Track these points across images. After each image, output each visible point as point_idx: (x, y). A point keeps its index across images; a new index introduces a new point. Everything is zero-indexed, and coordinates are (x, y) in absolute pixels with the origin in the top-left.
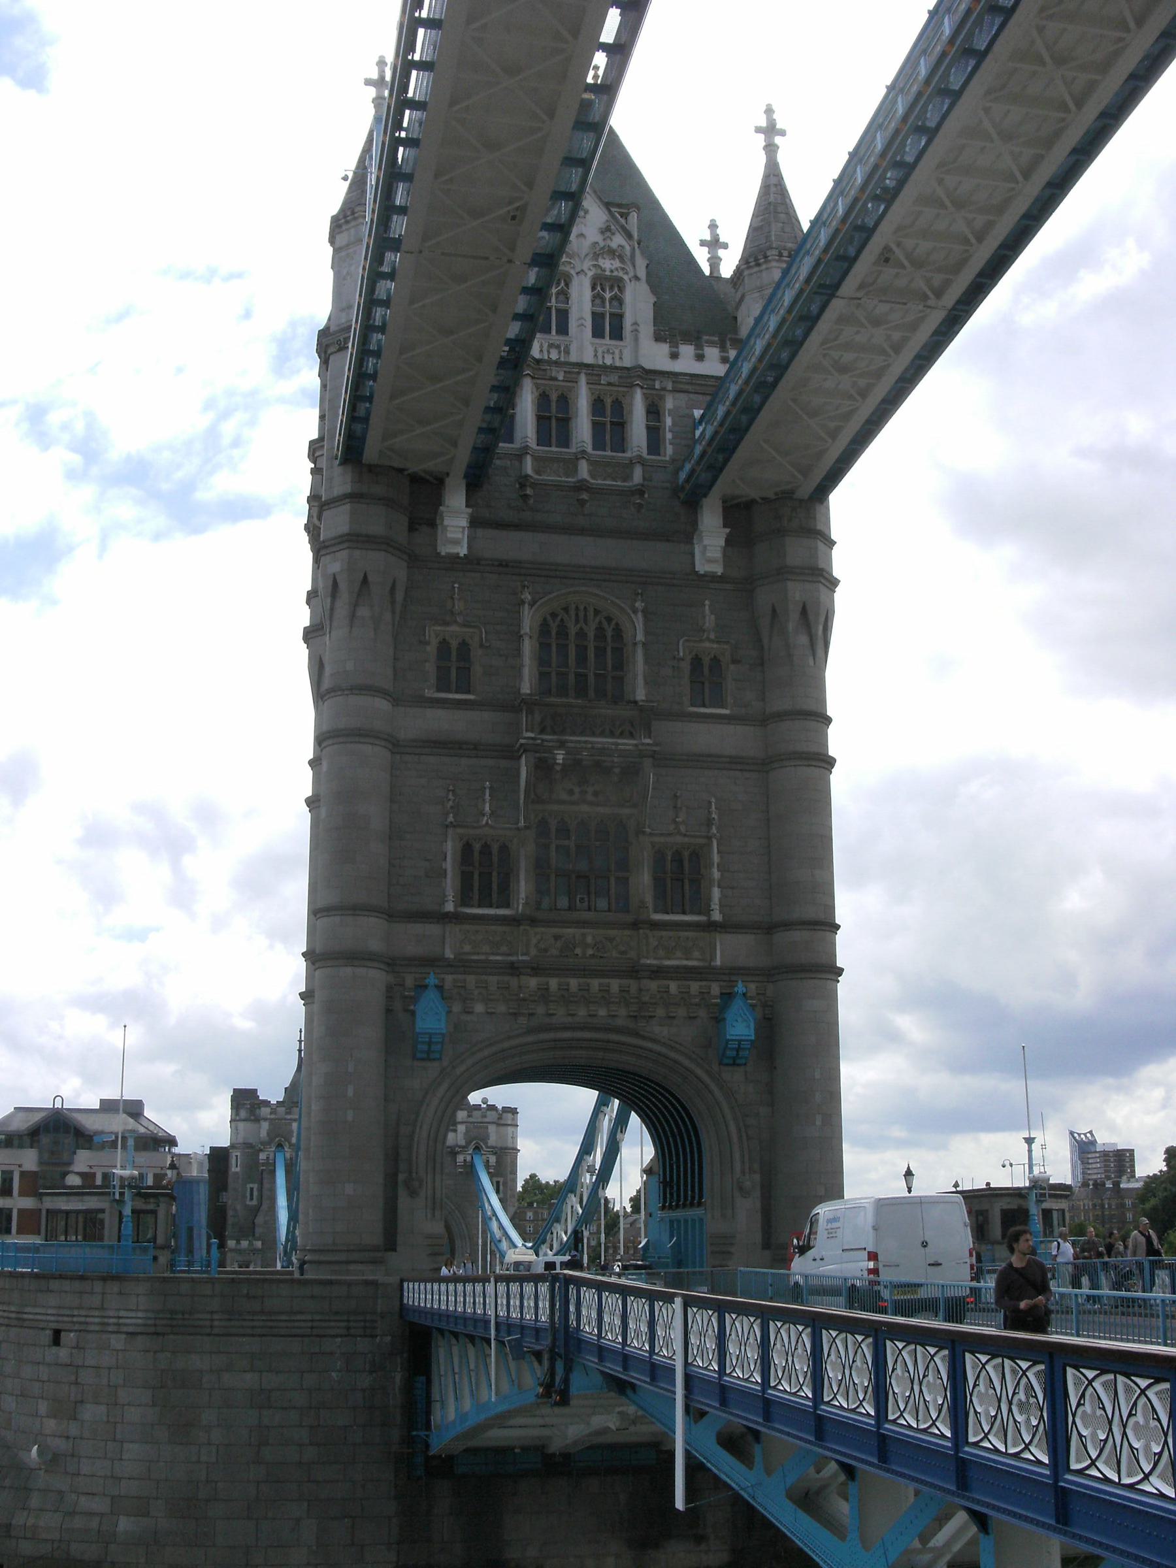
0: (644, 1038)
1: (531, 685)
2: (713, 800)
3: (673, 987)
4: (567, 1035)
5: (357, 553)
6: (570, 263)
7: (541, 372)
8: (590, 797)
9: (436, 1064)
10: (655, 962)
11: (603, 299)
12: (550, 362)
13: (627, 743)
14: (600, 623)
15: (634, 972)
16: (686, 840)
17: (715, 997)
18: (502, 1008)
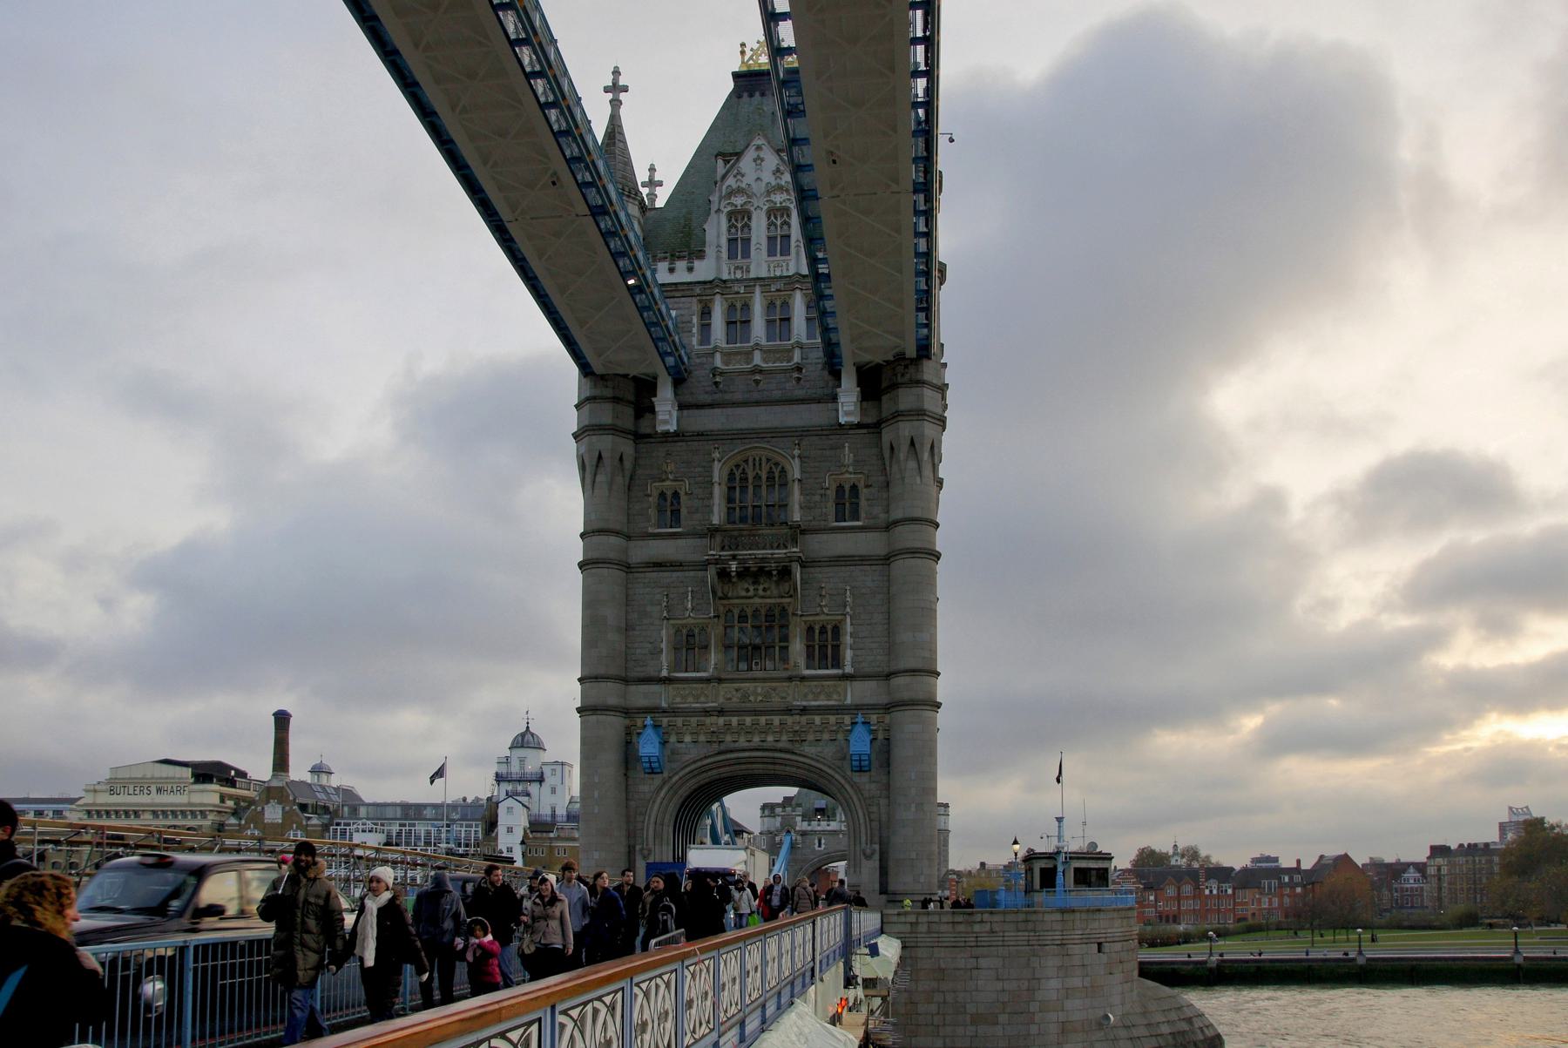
0: (796, 754)
1: (720, 517)
2: (848, 588)
3: (817, 719)
4: (747, 754)
6: (750, 202)
7: (728, 290)
8: (761, 592)
9: (660, 775)
10: (804, 703)
11: (776, 225)
12: (732, 281)
14: (771, 468)
15: (788, 711)
16: (829, 617)
18: (702, 738)
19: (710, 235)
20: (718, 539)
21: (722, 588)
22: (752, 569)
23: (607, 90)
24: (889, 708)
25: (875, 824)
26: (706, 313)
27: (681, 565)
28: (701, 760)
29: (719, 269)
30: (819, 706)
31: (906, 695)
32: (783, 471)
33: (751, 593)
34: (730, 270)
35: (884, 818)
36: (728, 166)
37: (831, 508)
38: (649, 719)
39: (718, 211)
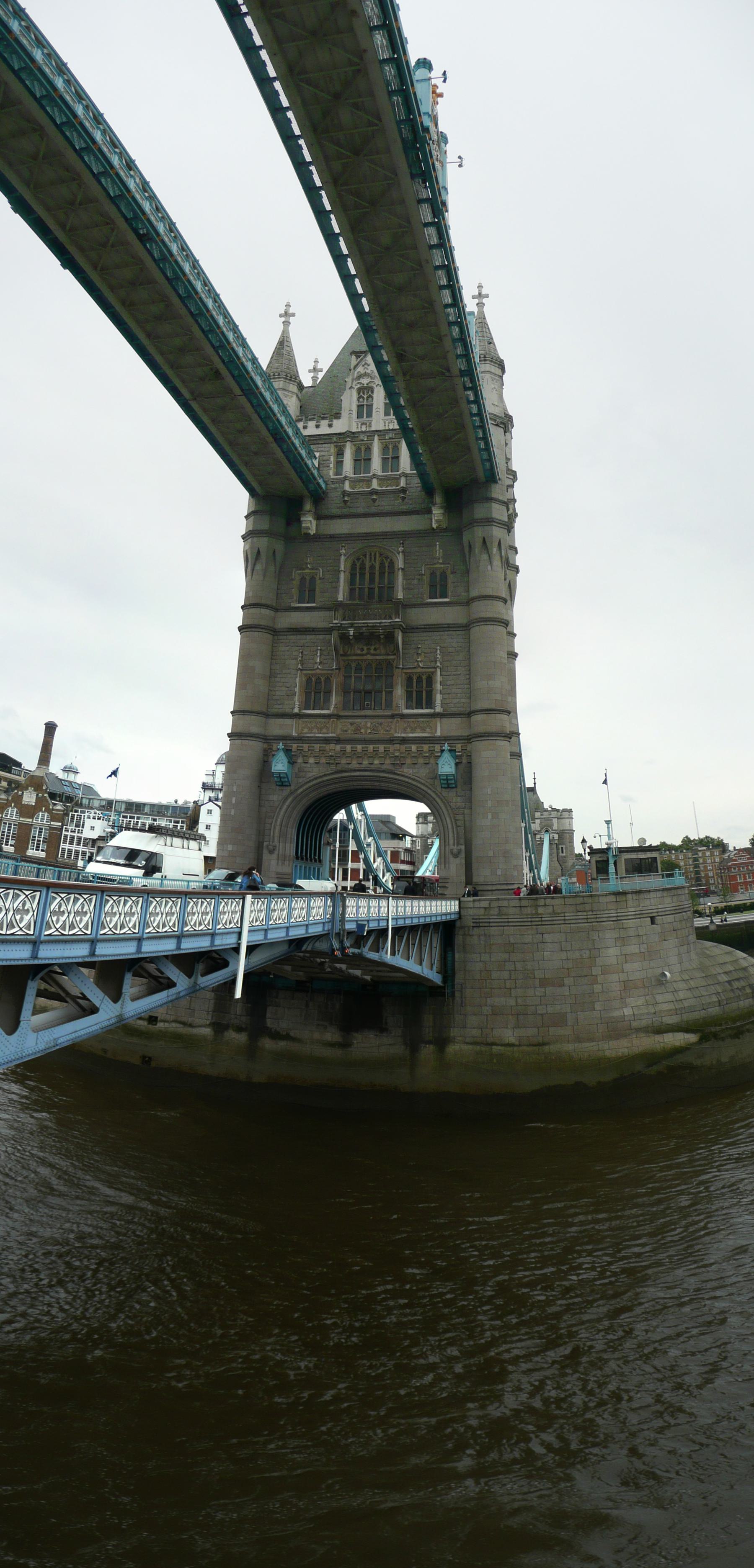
3: (414, 748)
8: (372, 651)
10: (403, 735)
12: (358, 432)
15: (391, 741)
16: (423, 670)
17: (438, 752)
18: (323, 760)
19: (345, 404)
20: (341, 612)
24: (469, 739)
26: (340, 453)
29: (350, 425)
30: (415, 737)
31: (482, 729)
33: (365, 652)
36: (359, 360)
37: (426, 589)
39: (351, 387)
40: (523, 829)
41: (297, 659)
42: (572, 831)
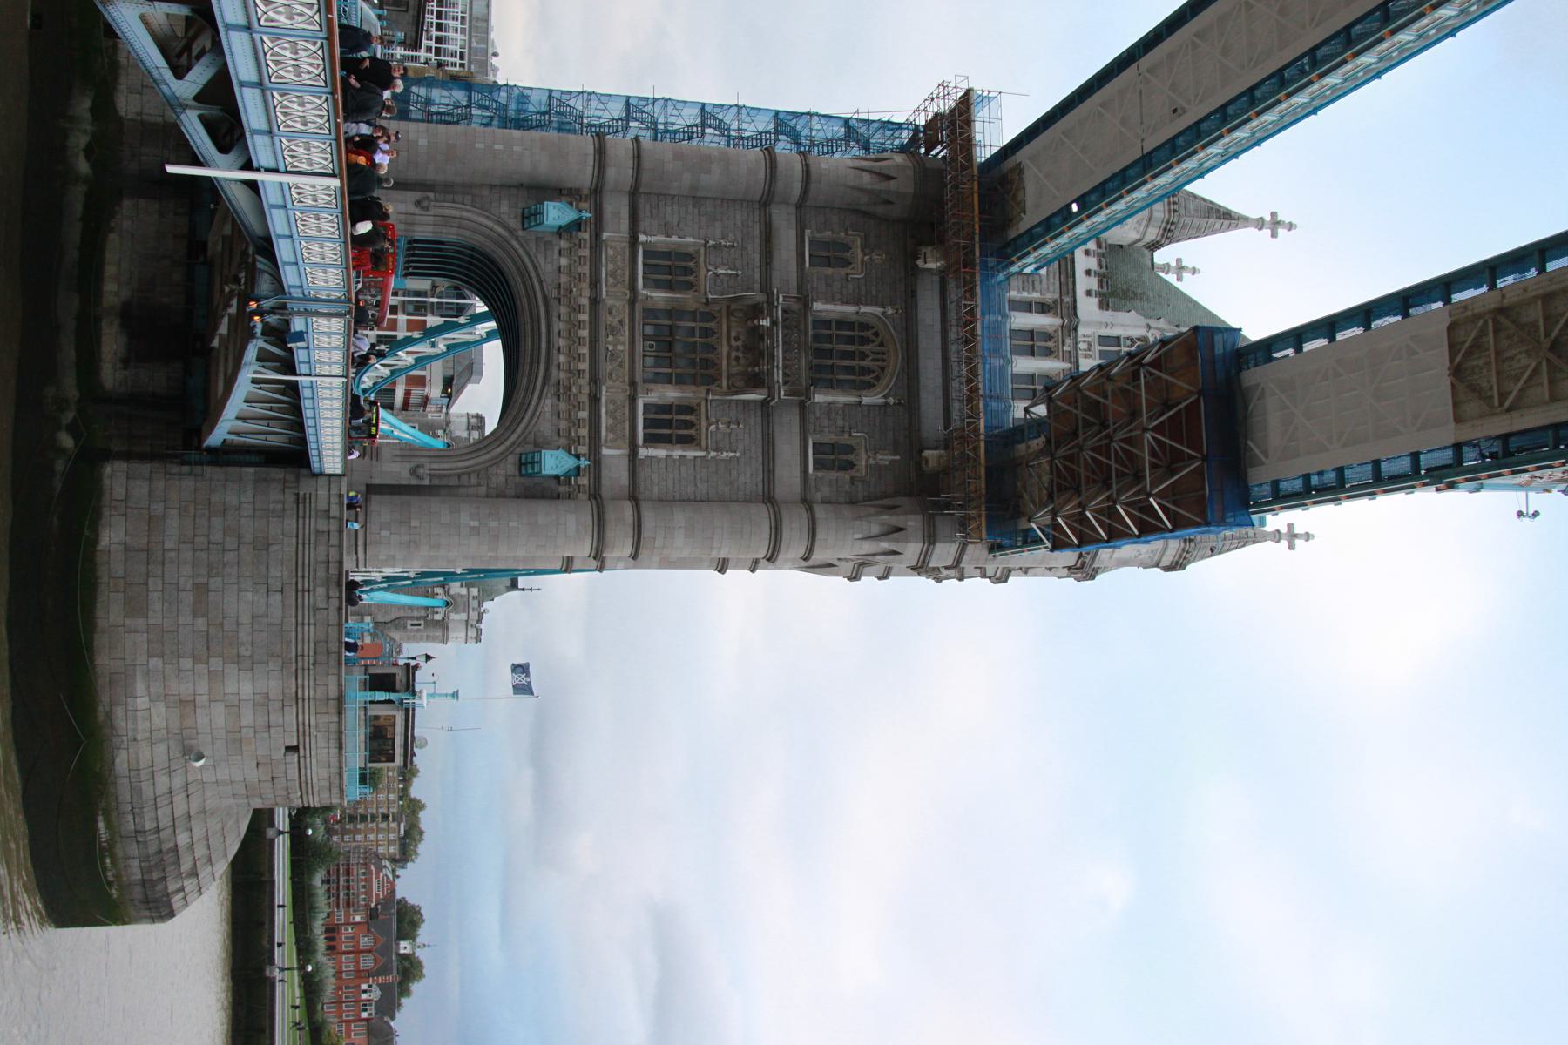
2: (738, 454)
3: (584, 414)
5: (910, 173)
8: (734, 354)
10: (603, 400)
12: (1076, 337)
13: (779, 376)
15: (595, 381)
16: (704, 431)
17: (576, 449)
18: (564, 279)
19: (1122, 317)
20: (796, 306)
21: (740, 310)
22: (761, 343)
23: (1273, 214)
24: (596, 496)
25: (455, 482)
26: (1044, 308)
27: (767, 263)
28: (538, 275)
29: (1088, 324)
30: (600, 416)
31: (610, 516)
32: (869, 386)
33: (733, 343)
34: (1088, 336)
35: (462, 491)
37: (829, 438)
38: (589, 215)
39: (1149, 327)
40: (452, 570)
41: (723, 239)
42: (445, 641)
